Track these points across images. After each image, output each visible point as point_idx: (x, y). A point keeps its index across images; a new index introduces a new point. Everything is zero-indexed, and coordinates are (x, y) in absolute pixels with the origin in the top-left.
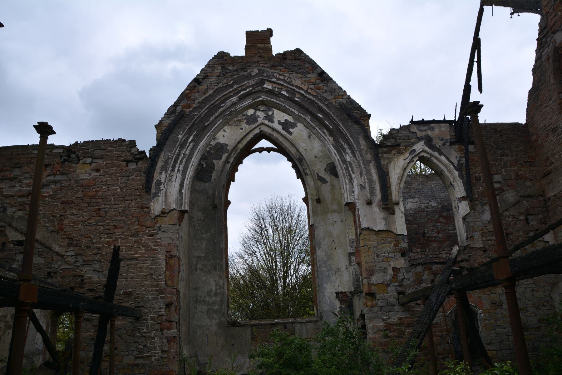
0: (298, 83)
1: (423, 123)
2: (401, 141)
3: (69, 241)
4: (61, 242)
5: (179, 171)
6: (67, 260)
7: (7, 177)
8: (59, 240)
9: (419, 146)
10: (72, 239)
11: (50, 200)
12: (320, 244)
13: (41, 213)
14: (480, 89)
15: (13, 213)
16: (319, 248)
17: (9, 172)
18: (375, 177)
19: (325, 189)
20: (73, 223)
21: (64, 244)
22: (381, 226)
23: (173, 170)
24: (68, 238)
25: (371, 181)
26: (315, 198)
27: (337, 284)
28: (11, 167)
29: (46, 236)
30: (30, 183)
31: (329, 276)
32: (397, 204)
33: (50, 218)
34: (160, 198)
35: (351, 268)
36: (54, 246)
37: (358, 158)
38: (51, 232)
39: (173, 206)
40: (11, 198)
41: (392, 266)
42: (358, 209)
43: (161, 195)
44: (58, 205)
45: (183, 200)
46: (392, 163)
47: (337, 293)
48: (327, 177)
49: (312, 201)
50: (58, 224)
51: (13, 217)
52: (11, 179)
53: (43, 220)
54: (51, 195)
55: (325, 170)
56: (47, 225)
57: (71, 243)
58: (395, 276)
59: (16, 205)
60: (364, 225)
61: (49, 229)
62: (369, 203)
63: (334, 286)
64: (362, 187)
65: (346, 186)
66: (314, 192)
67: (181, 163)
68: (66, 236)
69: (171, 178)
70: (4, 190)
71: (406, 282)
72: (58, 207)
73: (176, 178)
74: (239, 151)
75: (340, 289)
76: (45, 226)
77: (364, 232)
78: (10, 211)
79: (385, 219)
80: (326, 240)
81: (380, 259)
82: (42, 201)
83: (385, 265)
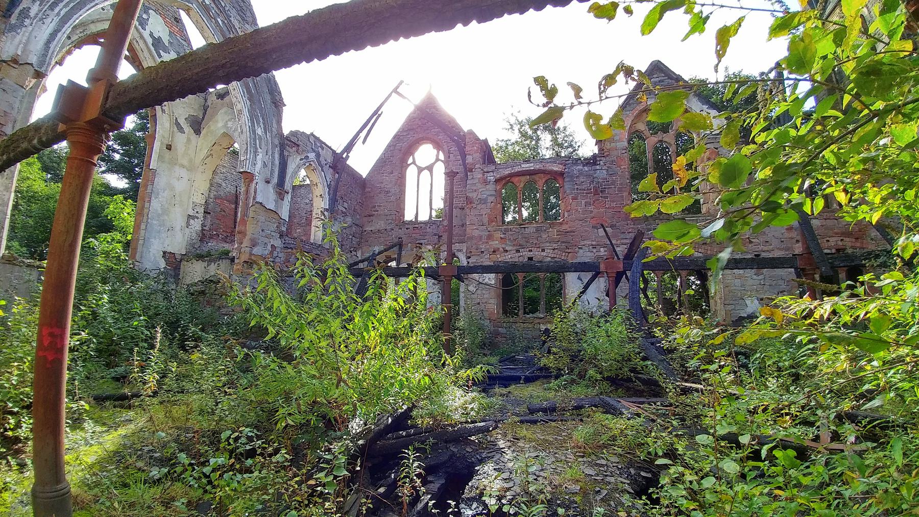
0: (237, 25)
1: (317, 139)
2: (301, 143)
5: (58, 14)
9: (312, 156)
12: (158, 194)
14: (364, 142)
16: (156, 198)
18: (277, 162)
19: (180, 140)
22: (271, 205)
23: (52, 8)
25: (273, 164)
26: (166, 142)
27: (167, 242)
31: (159, 232)
32: (288, 193)
34: (18, 38)
35: (187, 231)
37: (268, 137)
39: (33, 59)
41: (272, 243)
42: (257, 183)
43: (22, 33)
45: (48, 59)
46: (291, 158)
47: (164, 253)
48: (187, 129)
49: (162, 143)
55: (186, 119)
58: (272, 253)
60: (259, 199)
62: (268, 182)
63: (163, 244)
64: (265, 165)
65: (250, 156)
66: (166, 135)
67: (65, 6)
69: (44, 17)
71: (278, 260)
73: (51, 22)
74: (88, 33)
75: (169, 249)
77: (256, 204)
79: (276, 202)
80: (166, 192)
81: (264, 234)
83: (266, 240)
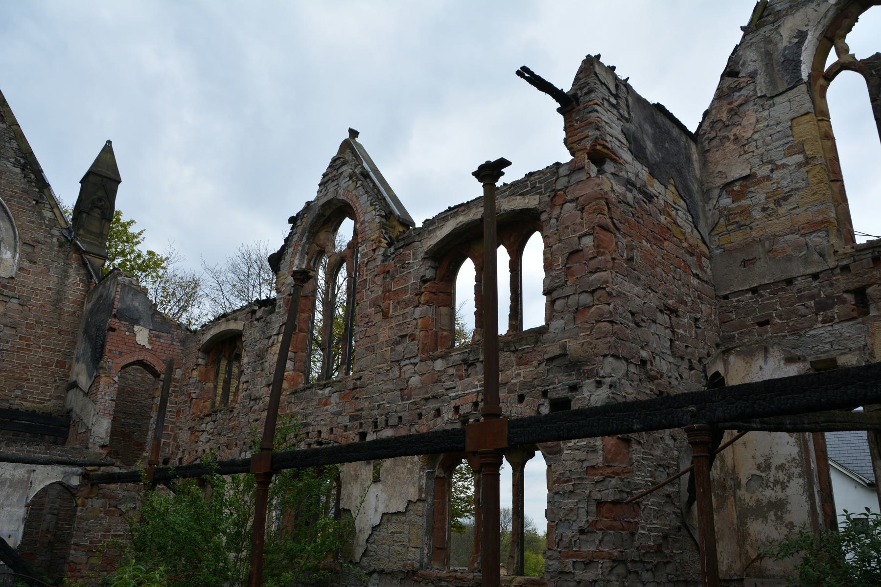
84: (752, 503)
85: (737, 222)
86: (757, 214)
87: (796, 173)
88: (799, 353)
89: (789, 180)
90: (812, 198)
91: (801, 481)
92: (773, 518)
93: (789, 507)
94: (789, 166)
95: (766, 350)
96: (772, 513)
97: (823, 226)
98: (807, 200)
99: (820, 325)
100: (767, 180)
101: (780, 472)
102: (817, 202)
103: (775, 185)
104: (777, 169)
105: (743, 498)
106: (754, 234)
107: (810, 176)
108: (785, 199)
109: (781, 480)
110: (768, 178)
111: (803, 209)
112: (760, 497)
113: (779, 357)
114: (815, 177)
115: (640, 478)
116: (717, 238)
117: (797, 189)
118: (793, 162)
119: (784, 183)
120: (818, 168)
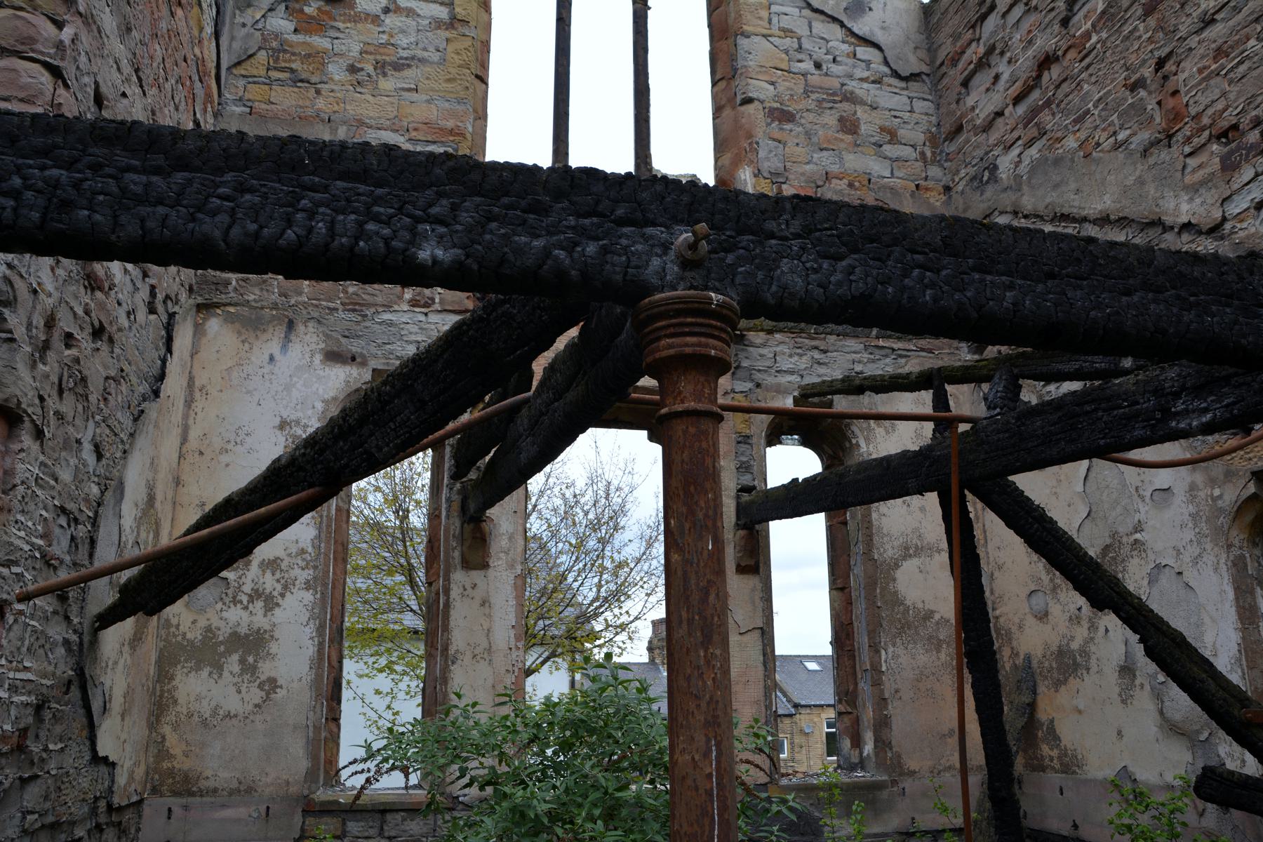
3: (1226, 144)
4: (1194, 171)
6: (1242, 234)
7: (972, 66)
8: (1184, 167)
10: (1235, 127)
11: (1104, 35)
13: (1090, 105)
15: (1016, 167)
17: (974, 45)
20: (1220, 53)
21: (1208, 170)
24: (1218, 137)
28: (973, 27)
29: (1130, 181)
30: (1030, 32)
33: (1126, 100)
36: (1172, 205)
38: (1145, 153)
40: (1000, 120)
44: (1136, 29)
50: (1159, 103)
51: (1018, 177)
52: (983, 63)
53: (1104, 130)
54: (1103, 12)
56: (1122, 136)
57: (1238, 148)
59: (1015, 134)
61: (1133, 146)
68: (1207, 133)
70: (977, 111)
72: (1140, 37)
76: (1117, 146)
78: (1005, 163)
82: (1081, 61)
84: (195, 635)
85: (292, 71)
86: (336, 71)
87: (428, 34)
88: (355, 347)
89: (412, 40)
90: (444, 85)
91: (308, 596)
92: (236, 668)
93: (273, 648)
94: (419, 15)
95: (291, 325)
96: (235, 657)
97: (451, 138)
98: (436, 86)
99: (406, 307)
100: (373, 22)
101: (268, 574)
102: (452, 95)
103: (385, 37)
104: (395, 12)
105: (174, 621)
106: (320, 103)
107: (450, 49)
108: (398, 67)
109: (267, 591)
110: (376, 19)
111: (424, 97)
112: (215, 622)
113: (314, 346)
114: (458, 54)
115: (22, 534)
116: (241, 82)
117: (422, 61)
118: (428, 14)
119: (403, 41)
120: (468, 42)
